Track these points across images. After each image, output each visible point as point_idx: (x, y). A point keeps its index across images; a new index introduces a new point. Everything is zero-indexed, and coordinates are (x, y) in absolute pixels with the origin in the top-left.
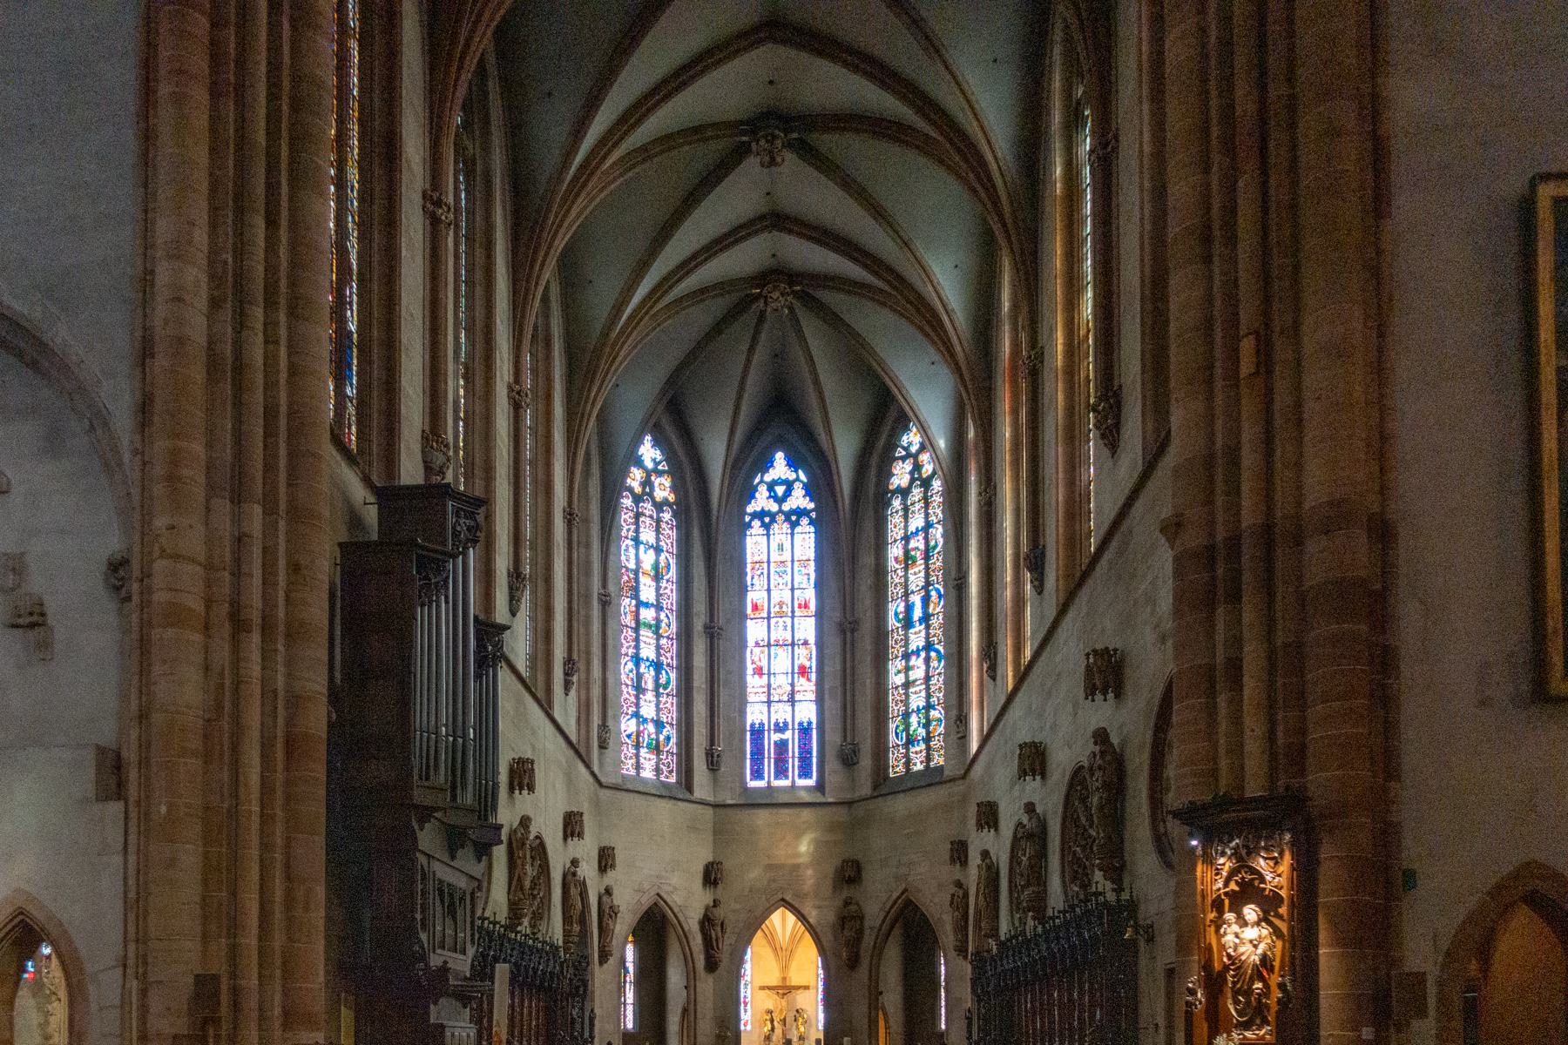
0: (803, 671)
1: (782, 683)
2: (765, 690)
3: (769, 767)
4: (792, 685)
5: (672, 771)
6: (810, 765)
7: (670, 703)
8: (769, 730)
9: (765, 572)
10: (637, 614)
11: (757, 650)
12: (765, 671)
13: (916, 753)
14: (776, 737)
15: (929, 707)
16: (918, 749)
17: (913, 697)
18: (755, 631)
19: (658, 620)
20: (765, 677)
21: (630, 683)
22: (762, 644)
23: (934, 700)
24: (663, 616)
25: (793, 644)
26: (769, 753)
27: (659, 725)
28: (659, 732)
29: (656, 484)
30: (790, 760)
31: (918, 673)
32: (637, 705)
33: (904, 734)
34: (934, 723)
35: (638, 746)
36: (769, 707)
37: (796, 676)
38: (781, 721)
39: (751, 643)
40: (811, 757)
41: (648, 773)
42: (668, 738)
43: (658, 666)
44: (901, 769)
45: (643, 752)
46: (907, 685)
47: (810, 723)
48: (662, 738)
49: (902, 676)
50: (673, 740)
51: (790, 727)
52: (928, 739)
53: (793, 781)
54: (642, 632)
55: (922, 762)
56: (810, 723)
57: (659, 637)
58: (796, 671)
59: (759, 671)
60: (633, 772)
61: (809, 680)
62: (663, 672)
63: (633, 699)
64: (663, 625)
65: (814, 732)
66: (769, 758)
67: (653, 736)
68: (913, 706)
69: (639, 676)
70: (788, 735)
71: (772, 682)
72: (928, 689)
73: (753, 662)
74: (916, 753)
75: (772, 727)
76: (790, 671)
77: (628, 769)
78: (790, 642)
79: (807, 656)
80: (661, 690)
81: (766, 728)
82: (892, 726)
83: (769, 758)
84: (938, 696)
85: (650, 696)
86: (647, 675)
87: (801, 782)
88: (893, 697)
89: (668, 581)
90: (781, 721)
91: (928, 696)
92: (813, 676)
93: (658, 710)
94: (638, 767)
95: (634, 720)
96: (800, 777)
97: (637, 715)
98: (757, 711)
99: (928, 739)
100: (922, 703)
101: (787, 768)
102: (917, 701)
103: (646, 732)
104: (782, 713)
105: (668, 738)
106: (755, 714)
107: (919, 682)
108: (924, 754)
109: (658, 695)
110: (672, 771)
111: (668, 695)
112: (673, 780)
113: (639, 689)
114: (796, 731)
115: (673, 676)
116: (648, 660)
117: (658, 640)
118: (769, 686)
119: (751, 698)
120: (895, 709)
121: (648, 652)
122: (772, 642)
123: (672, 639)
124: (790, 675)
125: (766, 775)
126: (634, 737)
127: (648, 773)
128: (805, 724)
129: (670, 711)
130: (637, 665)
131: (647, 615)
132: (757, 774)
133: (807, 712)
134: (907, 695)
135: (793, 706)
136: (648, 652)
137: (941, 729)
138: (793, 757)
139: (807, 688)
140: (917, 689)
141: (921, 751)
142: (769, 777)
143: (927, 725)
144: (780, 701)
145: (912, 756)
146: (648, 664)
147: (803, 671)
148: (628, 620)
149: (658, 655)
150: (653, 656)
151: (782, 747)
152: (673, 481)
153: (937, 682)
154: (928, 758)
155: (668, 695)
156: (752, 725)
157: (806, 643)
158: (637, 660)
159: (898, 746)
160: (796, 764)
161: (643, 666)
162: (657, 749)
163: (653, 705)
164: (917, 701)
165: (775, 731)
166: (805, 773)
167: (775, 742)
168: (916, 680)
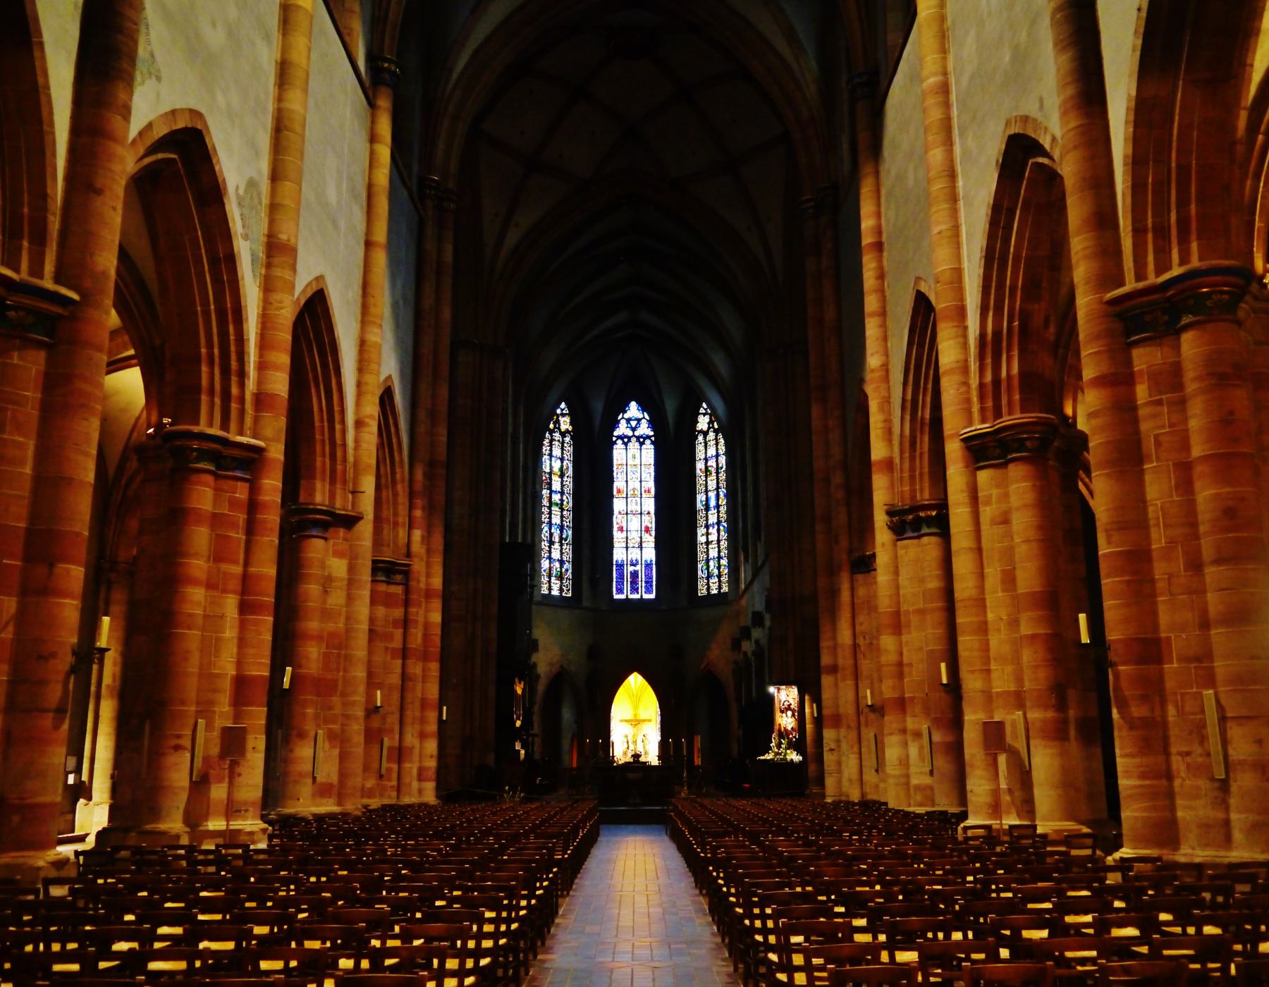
0: (647, 530)
1: (634, 537)
2: (625, 540)
3: (627, 586)
4: (641, 538)
5: (569, 590)
6: (652, 586)
7: (568, 549)
8: (627, 564)
9: (625, 471)
10: (550, 498)
11: (620, 516)
12: (625, 529)
13: (713, 583)
14: (631, 569)
15: (719, 558)
16: (714, 581)
17: (711, 551)
18: (618, 505)
19: (562, 500)
20: (625, 533)
21: (545, 539)
22: (623, 513)
23: (722, 554)
24: (564, 498)
25: (641, 514)
26: (627, 578)
27: (562, 562)
28: (561, 567)
29: (561, 422)
30: (640, 583)
31: (713, 537)
32: (550, 552)
33: (706, 571)
34: (723, 567)
35: (550, 576)
36: (627, 550)
37: (643, 532)
38: (634, 559)
39: (616, 512)
40: (652, 582)
41: (555, 592)
42: (567, 570)
43: (561, 528)
44: (705, 592)
45: (553, 579)
46: (708, 543)
47: (651, 561)
48: (563, 570)
49: (705, 537)
50: (570, 571)
51: (640, 563)
52: (719, 576)
53: (642, 596)
54: (553, 509)
55: (716, 589)
56: (651, 561)
57: (562, 510)
58: (643, 529)
59: (621, 529)
60: (547, 592)
61: (651, 535)
62: (565, 531)
63: (547, 548)
64: (565, 503)
65: (654, 566)
66: (627, 581)
67: (559, 570)
68: (711, 556)
69: (551, 534)
70: (638, 567)
71: (629, 536)
72: (719, 547)
73: (617, 524)
74: (713, 583)
75: (629, 563)
76: (639, 529)
77: (545, 591)
78: (639, 512)
79: (650, 521)
80: (563, 542)
81: (625, 563)
82: (699, 566)
83: (627, 581)
84: (724, 552)
85: (557, 546)
86: (555, 534)
87: (646, 596)
88: (701, 549)
89: (568, 477)
90: (634, 559)
91: (719, 552)
92: (653, 533)
93: (562, 553)
94: (550, 589)
95: (548, 561)
96: (645, 592)
97: (550, 558)
98: (620, 553)
99: (719, 576)
100: (716, 555)
101: (638, 588)
102: (713, 553)
103: (554, 567)
104: (634, 554)
105: (567, 570)
106: (618, 554)
107: (714, 543)
108: (717, 584)
109: (561, 545)
110: (569, 590)
111: (567, 544)
112: (570, 595)
113: (551, 543)
114: (643, 566)
115: (570, 533)
116: (556, 524)
117: (562, 512)
118: (627, 538)
119: (616, 545)
120: (701, 556)
121: (556, 520)
122: (629, 512)
123: (570, 511)
124: (639, 532)
125: (625, 591)
126: (547, 571)
127: (555, 592)
128: (649, 562)
129: (568, 556)
130: (550, 529)
131: (556, 498)
132: (620, 591)
133: (650, 554)
134: (707, 548)
135: (641, 550)
136: (556, 520)
137: (726, 571)
138: (642, 581)
139: (650, 541)
140: (713, 546)
141: (716, 583)
142: (627, 592)
143: (719, 568)
144: (633, 547)
145: (711, 585)
146: (556, 527)
147: (647, 530)
148: (545, 502)
149: (562, 521)
150: (559, 522)
151: (635, 575)
152: (571, 419)
153: (724, 544)
154: (720, 587)
155: (567, 544)
156: (616, 561)
157: (649, 513)
158: (550, 524)
159: (703, 578)
160: (644, 585)
161: (553, 528)
162: (560, 578)
163: (559, 551)
164: (713, 553)
165: (631, 565)
166: (648, 591)
167: (631, 572)
168: (712, 541)
